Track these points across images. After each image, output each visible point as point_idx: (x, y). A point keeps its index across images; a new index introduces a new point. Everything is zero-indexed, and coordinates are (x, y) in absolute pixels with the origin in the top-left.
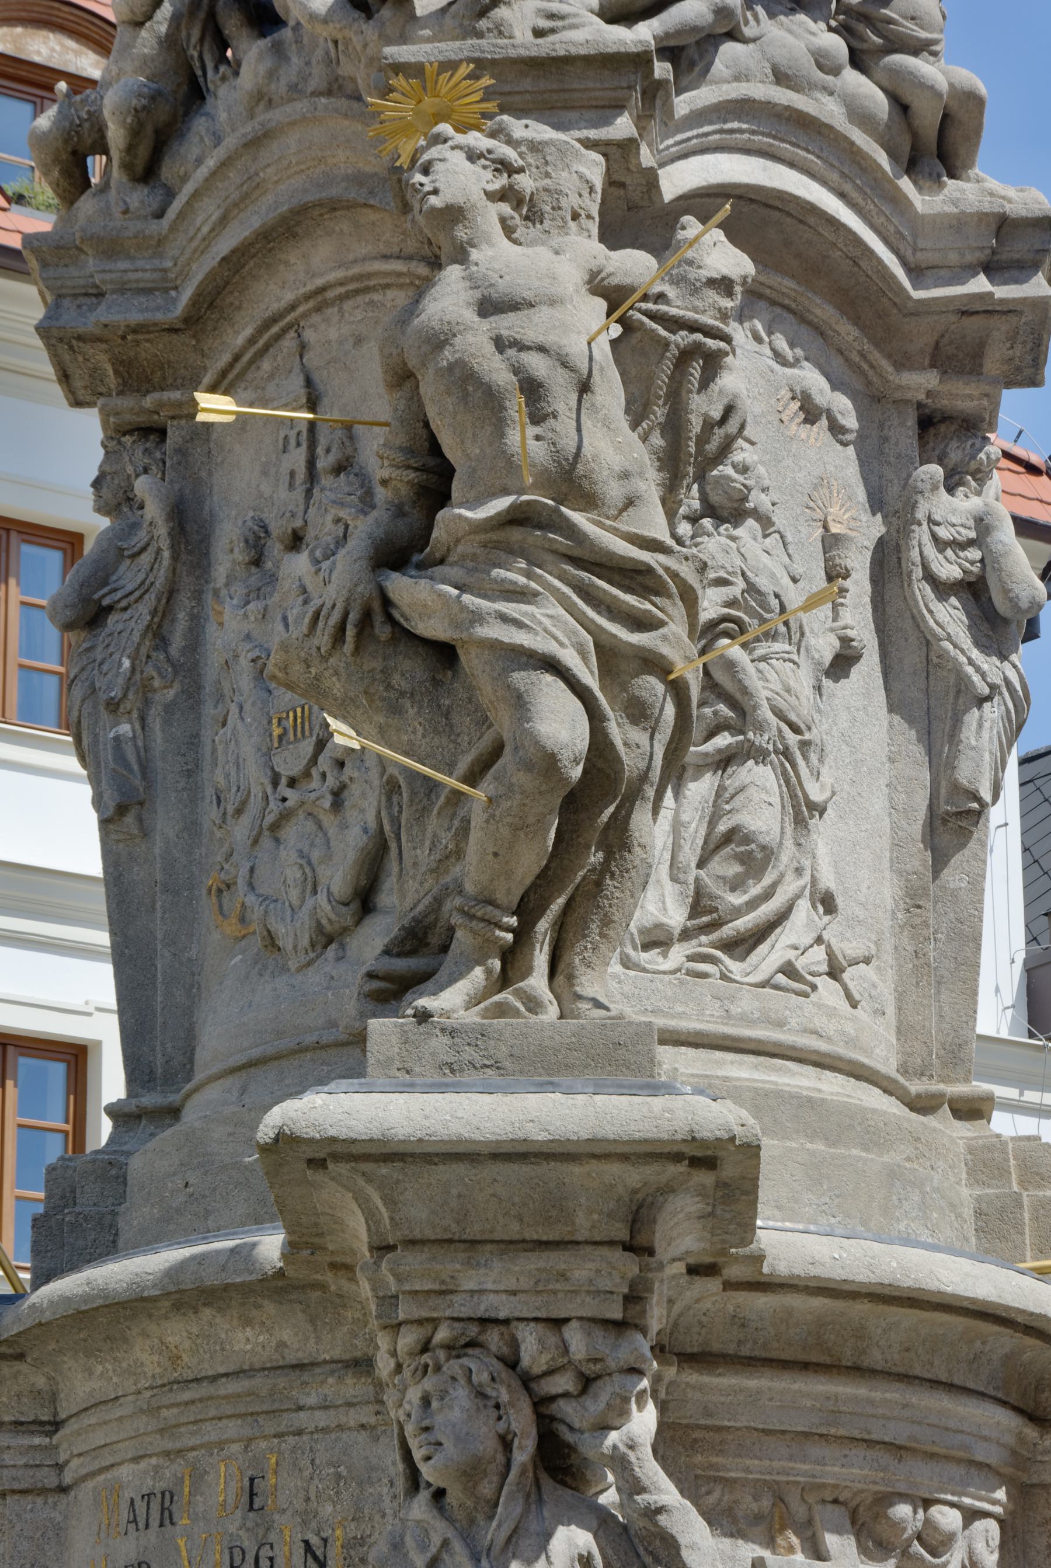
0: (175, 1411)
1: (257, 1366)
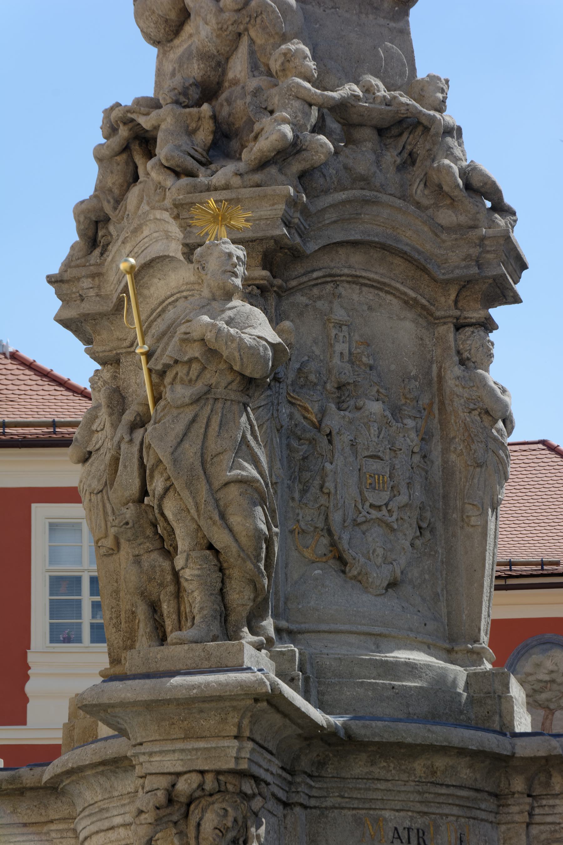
0: (432, 796)
1: (467, 786)
